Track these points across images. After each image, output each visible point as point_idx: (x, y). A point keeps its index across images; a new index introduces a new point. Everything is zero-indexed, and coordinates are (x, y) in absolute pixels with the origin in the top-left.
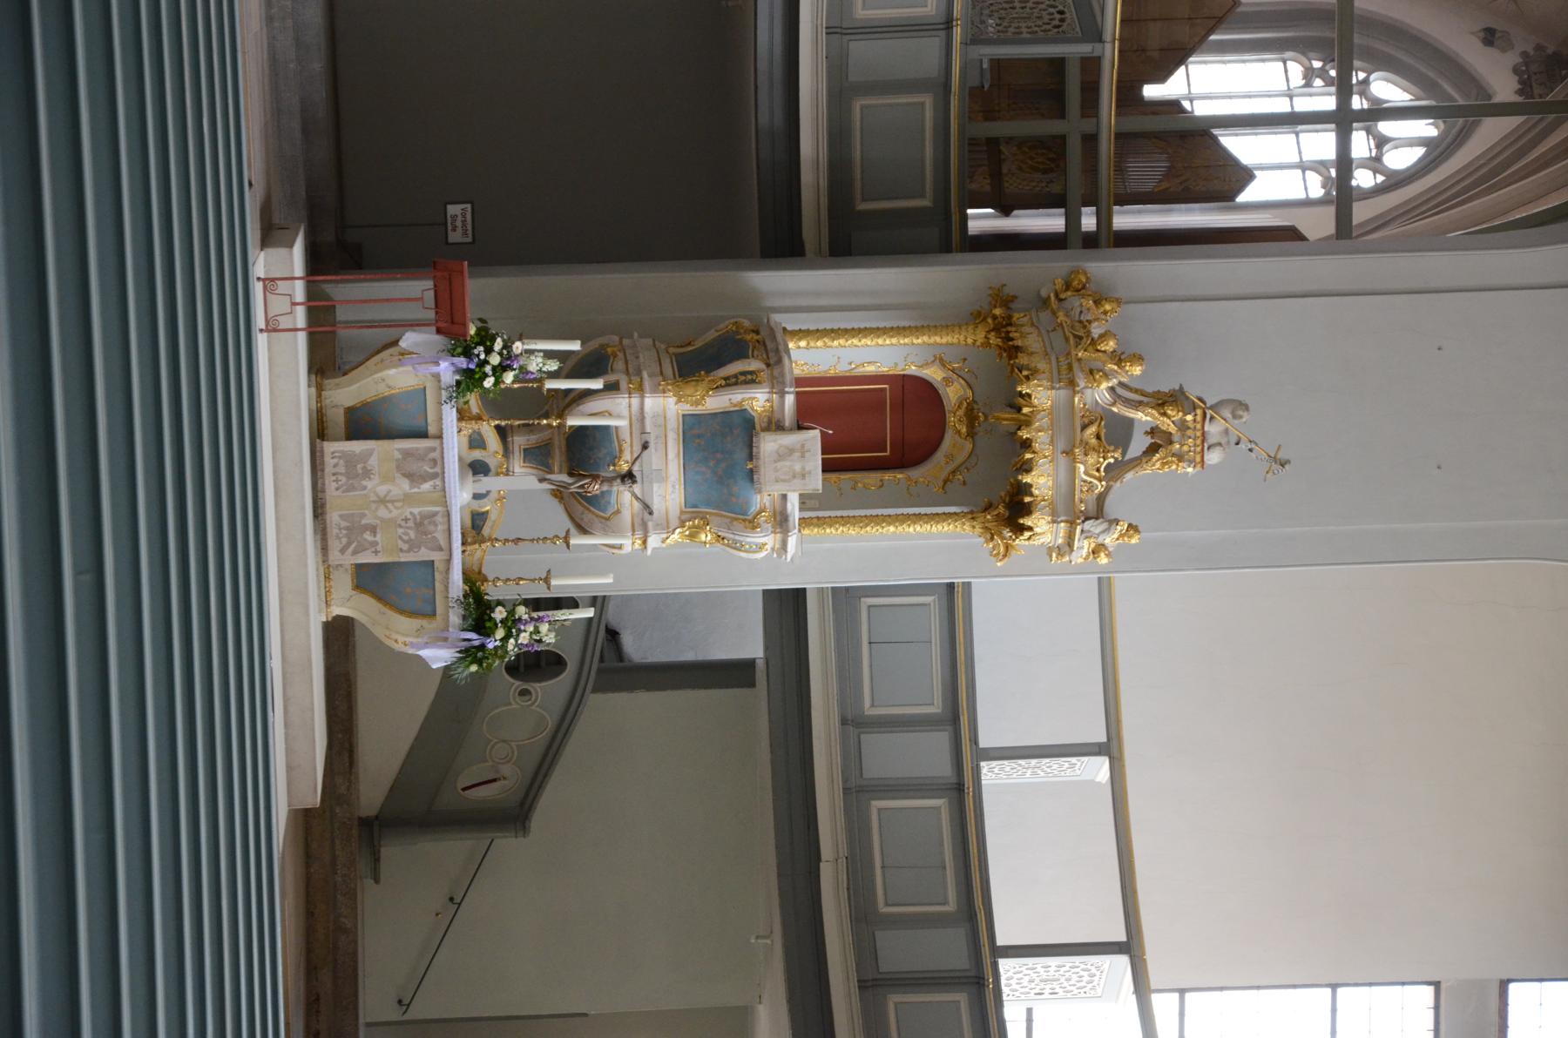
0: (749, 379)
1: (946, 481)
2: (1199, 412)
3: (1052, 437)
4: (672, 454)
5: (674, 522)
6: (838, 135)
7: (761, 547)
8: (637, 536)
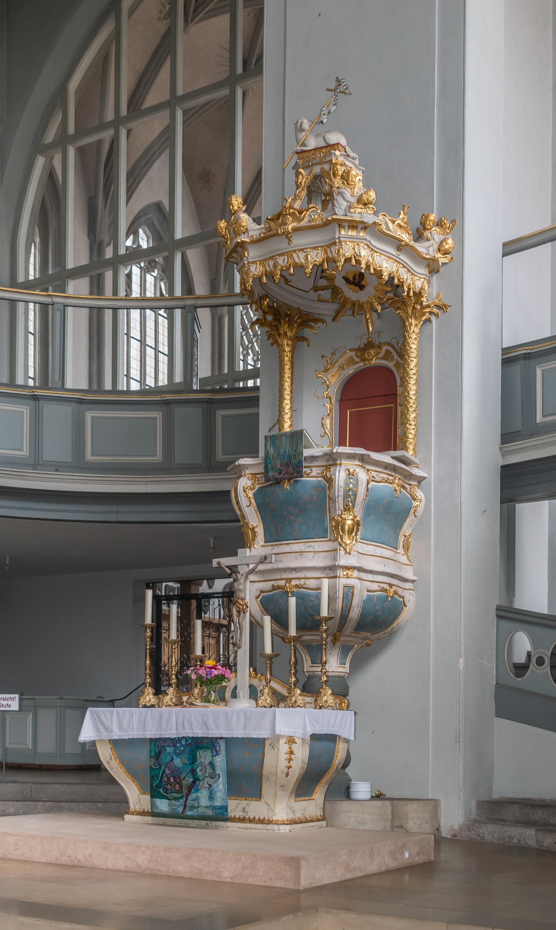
4: (286, 549)
5: (335, 545)
7: (350, 474)
8: (342, 574)
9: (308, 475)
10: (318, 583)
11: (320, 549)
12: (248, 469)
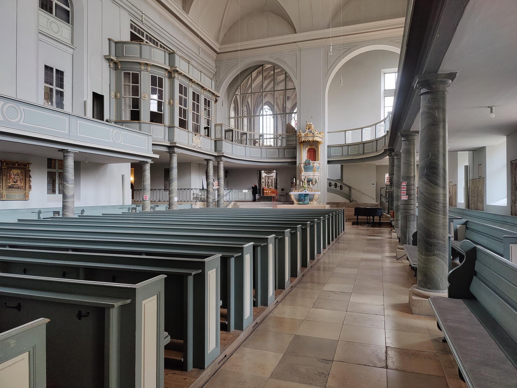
0: (301, 166)
6: (289, 158)
7: (316, 165)
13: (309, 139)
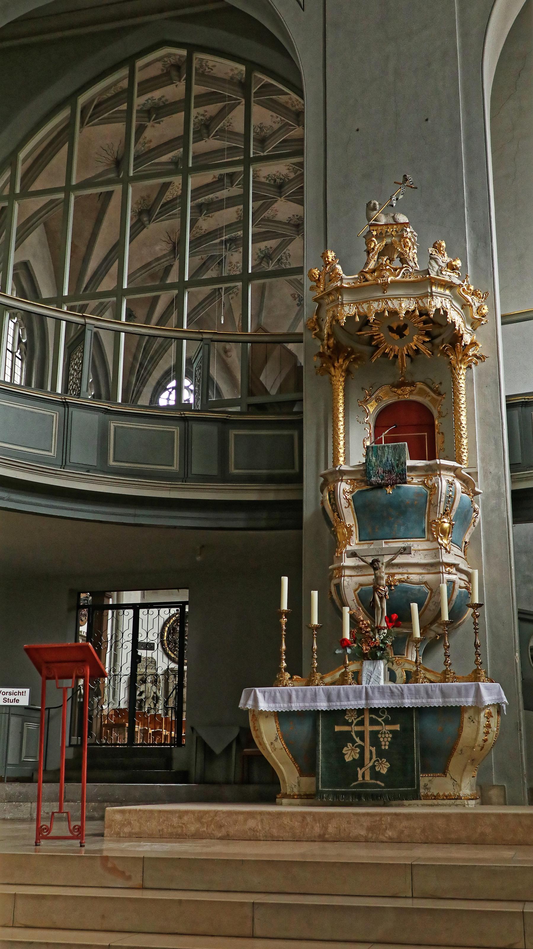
1: (439, 394)
2: (372, 228)
3: (374, 301)
5: (435, 545)
7: (451, 484)
8: (444, 571)
9: (410, 483)
10: (421, 577)
11: (420, 548)
12: (345, 475)
13: (393, 304)
